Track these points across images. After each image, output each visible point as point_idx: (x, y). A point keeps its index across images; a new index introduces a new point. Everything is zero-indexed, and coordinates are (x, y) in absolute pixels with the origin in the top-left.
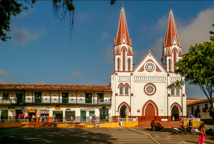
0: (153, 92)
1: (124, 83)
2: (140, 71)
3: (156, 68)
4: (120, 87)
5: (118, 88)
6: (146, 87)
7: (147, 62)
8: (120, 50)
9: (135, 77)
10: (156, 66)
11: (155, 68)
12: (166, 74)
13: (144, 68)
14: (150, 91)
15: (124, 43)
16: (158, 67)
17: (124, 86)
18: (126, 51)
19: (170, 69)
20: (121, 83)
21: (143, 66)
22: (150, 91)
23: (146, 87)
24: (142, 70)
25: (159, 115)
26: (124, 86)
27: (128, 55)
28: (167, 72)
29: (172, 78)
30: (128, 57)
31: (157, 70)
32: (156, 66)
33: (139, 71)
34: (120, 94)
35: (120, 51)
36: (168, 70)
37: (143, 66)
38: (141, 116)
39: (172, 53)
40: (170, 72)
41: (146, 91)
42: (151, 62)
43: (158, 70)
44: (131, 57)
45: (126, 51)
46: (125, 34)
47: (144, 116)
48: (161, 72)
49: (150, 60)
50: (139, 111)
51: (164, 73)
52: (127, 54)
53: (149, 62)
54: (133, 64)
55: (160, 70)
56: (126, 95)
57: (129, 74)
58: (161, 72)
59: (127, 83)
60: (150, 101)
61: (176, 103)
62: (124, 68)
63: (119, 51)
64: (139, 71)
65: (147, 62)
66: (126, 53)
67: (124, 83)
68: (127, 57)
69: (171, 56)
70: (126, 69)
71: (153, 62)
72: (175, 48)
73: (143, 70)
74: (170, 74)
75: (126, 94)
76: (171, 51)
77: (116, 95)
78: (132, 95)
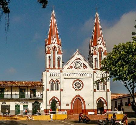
0: (81, 87)
1: (54, 80)
4: (51, 83)
5: (49, 84)
6: (74, 83)
8: (51, 49)
9: (65, 74)
10: (84, 63)
11: (83, 66)
12: (92, 71)
13: (73, 66)
15: (54, 43)
17: (54, 82)
18: (57, 50)
19: (96, 66)
20: (52, 80)
21: (72, 64)
23: (74, 83)
24: (70, 67)
26: (54, 82)
27: (58, 54)
29: (98, 75)
30: (58, 55)
32: (84, 63)
34: (51, 89)
35: (51, 50)
36: (94, 68)
37: (72, 64)
39: (98, 52)
40: (96, 69)
41: (75, 87)
42: (78, 60)
43: (85, 67)
44: (61, 56)
45: (57, 50)
46: (55, 35)
47: (73, 109)
49: (78, 59)
50: (68, 105)
51: (90, 71)
53: (77, 60)
54: (63, 62)
57: (59, 71)
59: (57, 80)
60: (78, 95)
61: (101, 97)
62: (54, 66)
66: (56, 52)
67: (54, 80)
68: (57, 56)
69: (97, 55)
70: (57, 67)
72: (100, 47)
73: (71, 67)
74: (96, 71)
75: (56, 89)
76: (97, 50)
77: (48, 90)
78: (62, 90)
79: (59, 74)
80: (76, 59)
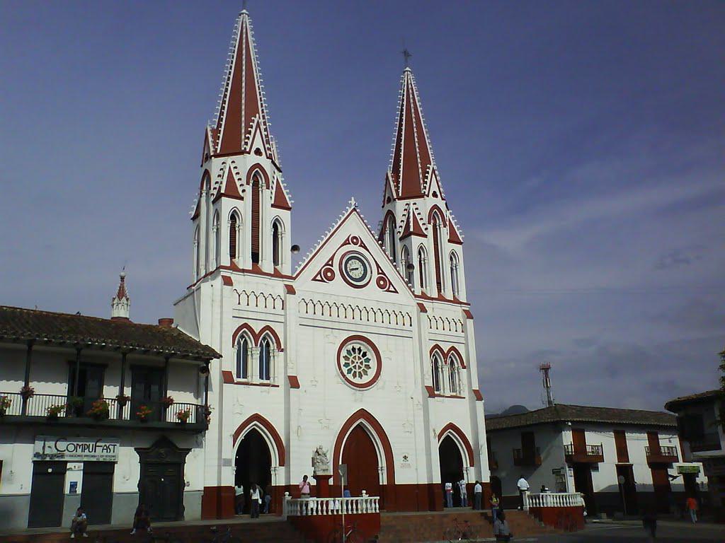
1: (257, 327)
2: (319, 278)
3: (379, 273)
4: (239, 343)
11: (375, 276)
12: (410, 305)
14: (357, 371)
20: (246, 325)
22: (360, 368)
24: (326, 275)
28: (416, 296)
31: (382, 283)
33: (314, 279)
39: (429, 223)
42: (357, 248)
43: (383, 283)
44: (285, 215)
48: (396, 292)
49: (355, 240)
51: (404, 300)
53: (351, 247)
54: (295, 248)
55: (390, 283)
56: (265, 382)
57: (278, 286)
58: (396, 292)
59: (268, 328)
60: (363, 413)
64: (314, 279)
67: (257, 327)
71: (365, 247)
73: (329, 274)
75: (261, 377)
76: (425, 215)
78: (294, 382)
79: (279, 304)
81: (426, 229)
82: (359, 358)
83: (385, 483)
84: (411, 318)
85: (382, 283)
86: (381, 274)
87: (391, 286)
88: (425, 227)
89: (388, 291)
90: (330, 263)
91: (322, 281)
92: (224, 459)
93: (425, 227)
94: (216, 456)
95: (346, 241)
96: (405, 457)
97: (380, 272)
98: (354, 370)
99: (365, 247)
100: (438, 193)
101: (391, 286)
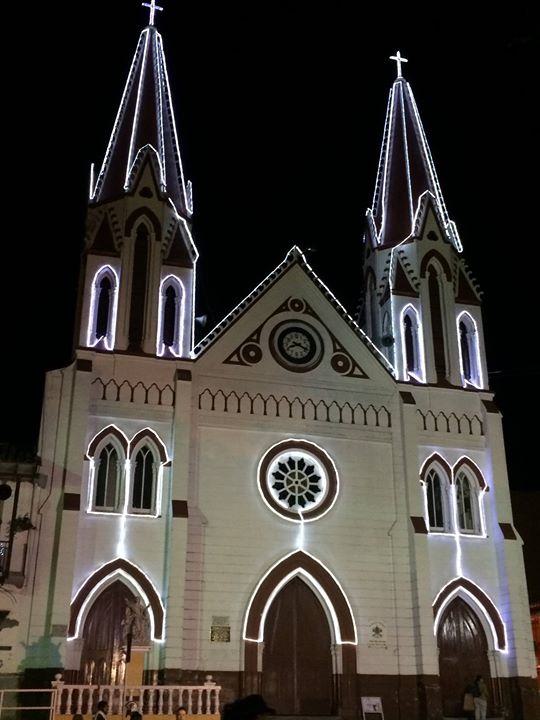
3: (335, 350)
7: (279, 310)
8: (121, 225)
10: (335, 340)
11: (329, 354)
13: (264, 345)
14: (297, 495)
16: (343, 349)
21: (258, 331)
24: (248, 354)
25: (361, 670)
31: (340, 364)
37: (258, 331)
38: (237, 670)
42: (300, 315)
45: (158, 238)
49: (297, 305)
52: (162, 251)
53: (291, 315)
63: (115, 235)
64: (227, 361)
65: (279, 310)
71: (314, 314)
73: (252, 354)
80: (282, 309)
81: (417, 285)
82: (301, 476)
83: (340, 671)
84: (389, 415)
85: (340, 364)
86: (339, 351)
87: (356, 369)
88: (416, 282)
89: (351, 375)
90: (255, 337)
91: (241, 363)
92: (54, 626)
93: (416, 282)
94: (43, 622)
95: (281, 307)
96: (377, 631)
97: (338, 347)
98: (291, 493)
99: (314, 314)
100: (438, 234)
101: (356, 369)
